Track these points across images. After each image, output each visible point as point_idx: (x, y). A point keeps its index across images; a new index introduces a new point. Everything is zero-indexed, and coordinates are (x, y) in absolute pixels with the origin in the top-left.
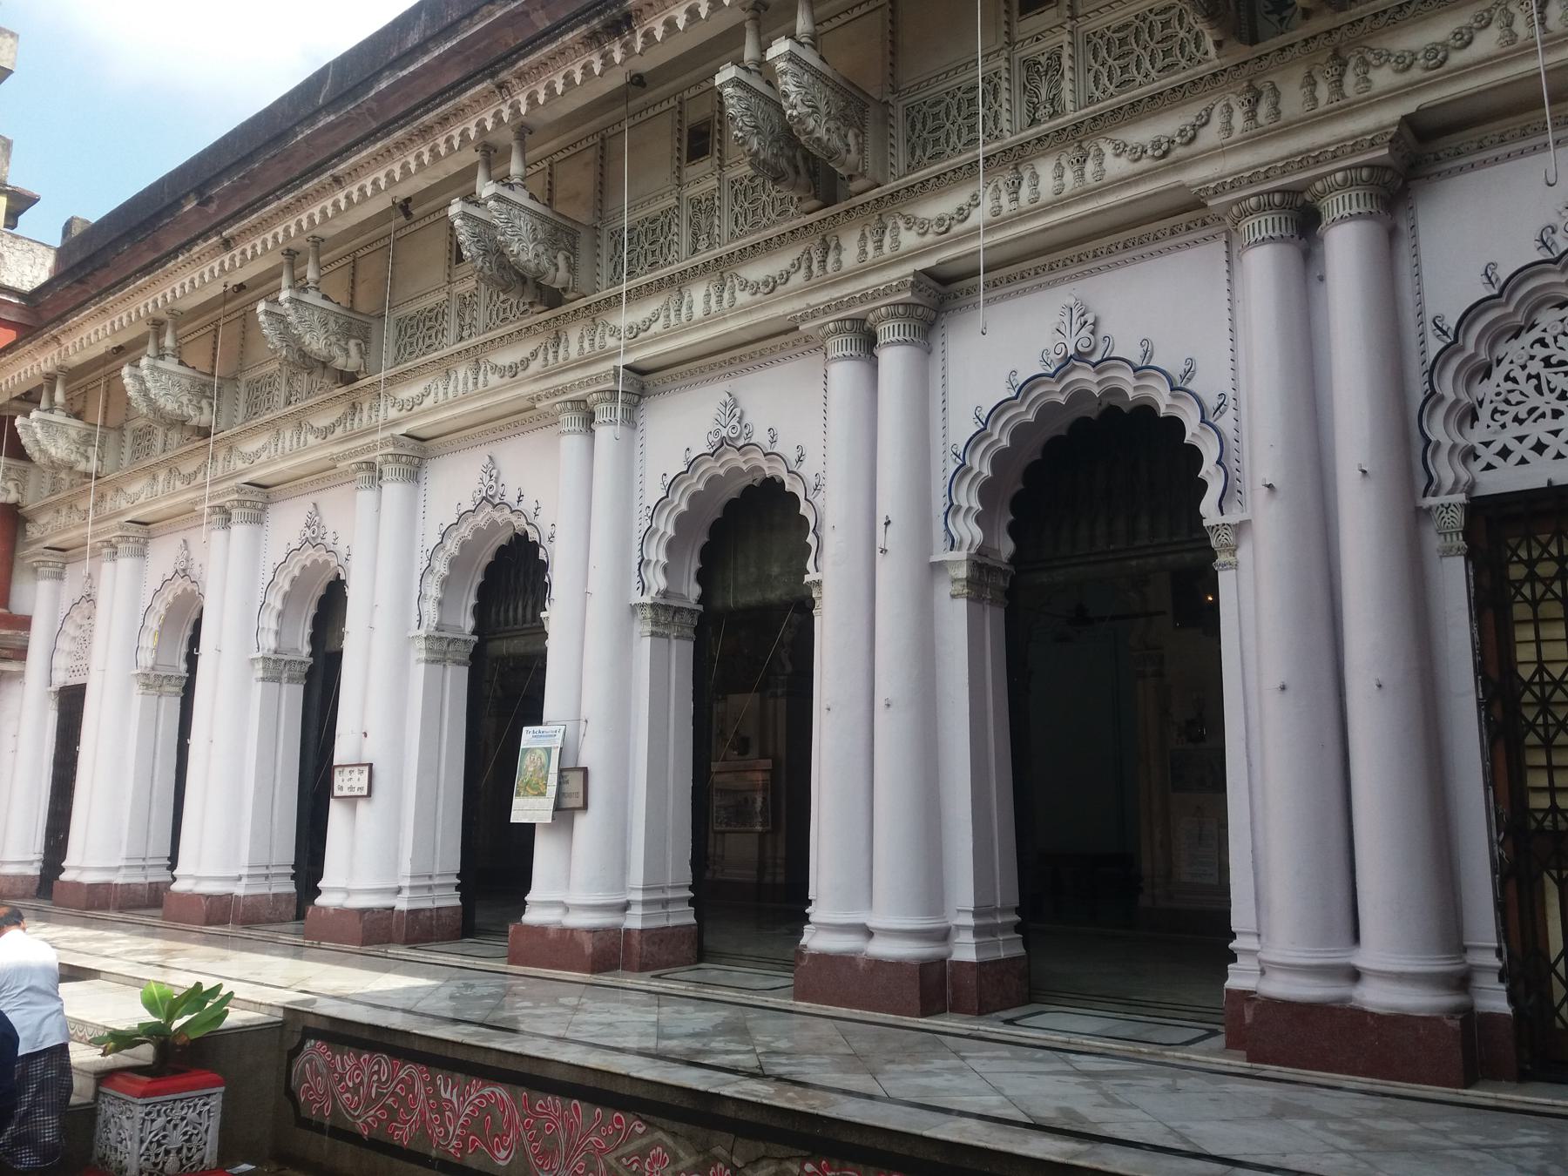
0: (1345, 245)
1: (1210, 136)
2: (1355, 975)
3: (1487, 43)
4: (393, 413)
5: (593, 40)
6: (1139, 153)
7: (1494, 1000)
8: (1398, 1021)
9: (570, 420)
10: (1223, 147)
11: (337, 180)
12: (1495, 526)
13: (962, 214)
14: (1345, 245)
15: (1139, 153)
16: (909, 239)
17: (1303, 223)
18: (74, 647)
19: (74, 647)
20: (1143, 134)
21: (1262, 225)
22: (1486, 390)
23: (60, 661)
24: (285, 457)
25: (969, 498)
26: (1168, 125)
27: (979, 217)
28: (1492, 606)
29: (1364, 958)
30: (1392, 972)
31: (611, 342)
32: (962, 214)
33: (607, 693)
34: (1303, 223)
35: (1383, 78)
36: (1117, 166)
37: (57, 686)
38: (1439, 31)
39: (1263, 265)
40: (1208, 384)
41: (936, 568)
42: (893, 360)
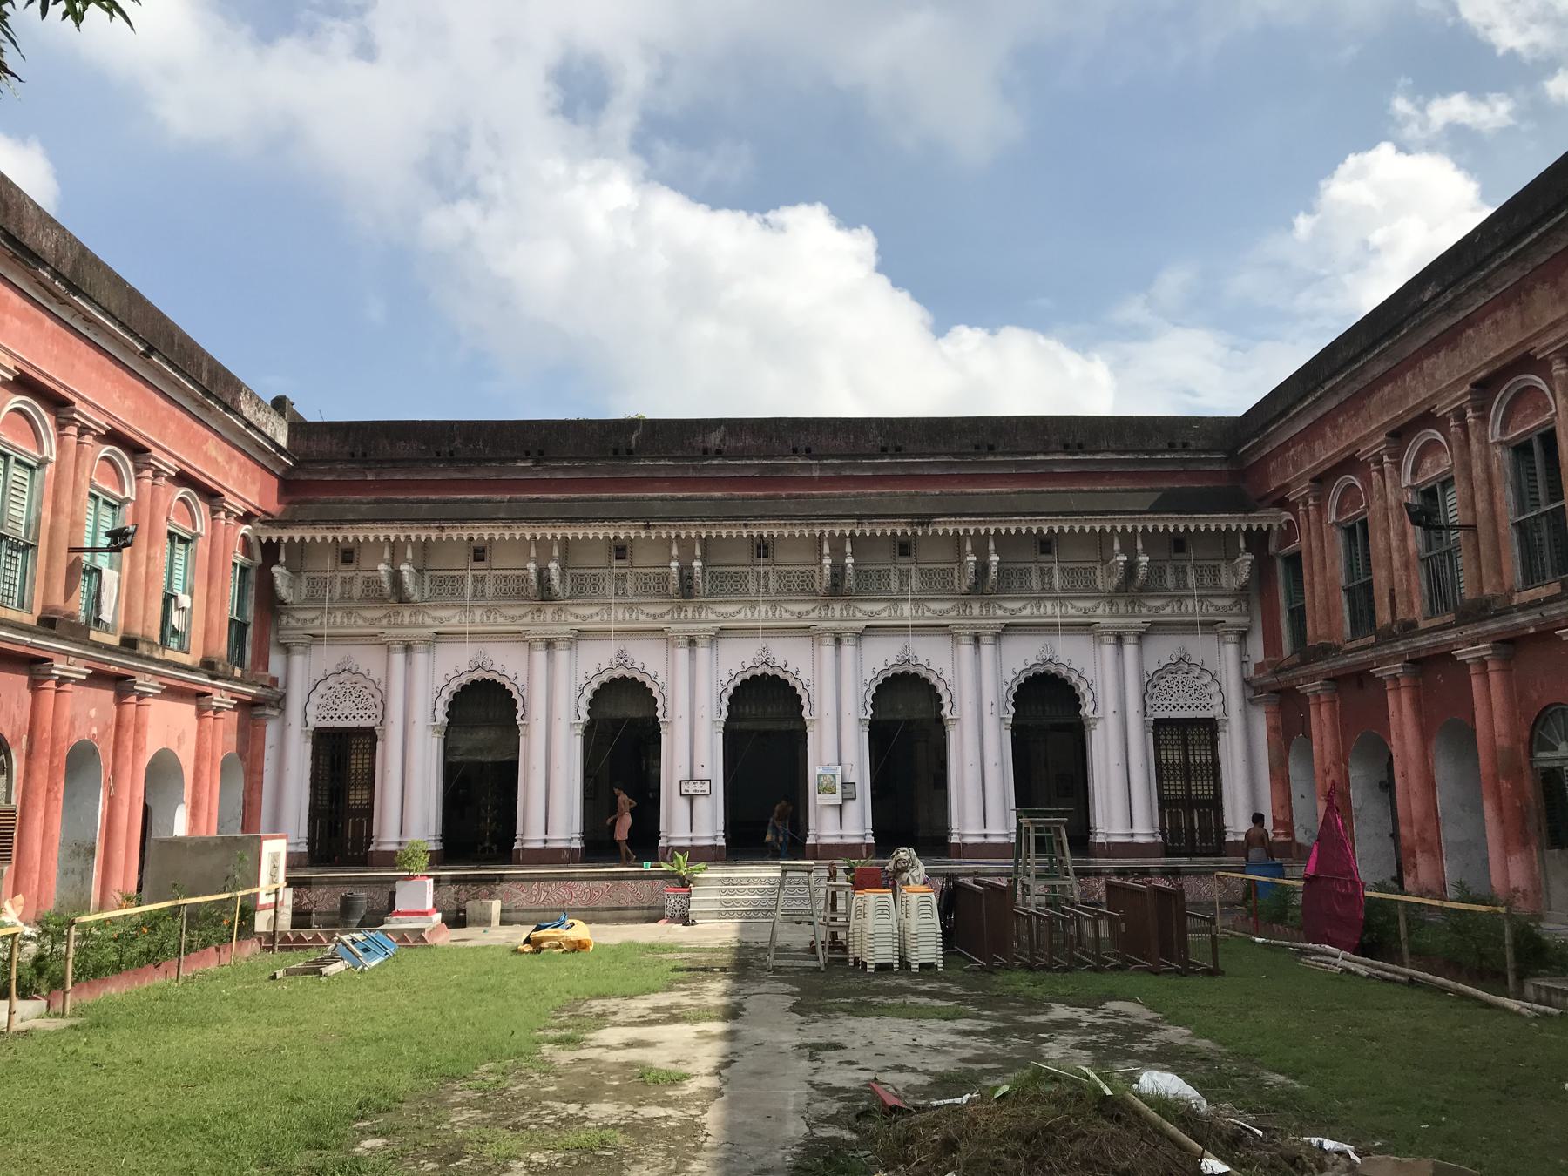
0: (1130, 649)
1: (1099, 611)
2: (1132, 835)
3: (1168, 610)
4: (712, 617)
5: (912, 524)
6: (1078, 610)
7: (1160, 839)
8: (1147, 844)
9: (831, 641)
10: (1103, 615)
11: (746, 526)
12: (1160, 725)
13: (1020, 610)
14: (1130, 649)
15: (1078, 610)
16: (1000, 613)
17: (1119, 639)
18: (323, 701)
19: (323, 701)
20: (1080, 604)
21: (1112, 639)
22: (1156, 690)
23: (311, 710)
24: (617, 621)
25: (1012, 699)
26: (1088, 604)
27: (1025, 613)
28: (1157, 744)
29: (1134, 831)
30: (1144, 830)
31: (859, 615)
32: (1020, 610)
33: (838, 752)
34: (1119, 639)
35: (1144, 610)
36: (1071, 611)
37: (311, 728)
38: (1158, 603)
39: (1108, 650)
40: (1088, 675)
41: (1002, 719)
42: (987, 650)
